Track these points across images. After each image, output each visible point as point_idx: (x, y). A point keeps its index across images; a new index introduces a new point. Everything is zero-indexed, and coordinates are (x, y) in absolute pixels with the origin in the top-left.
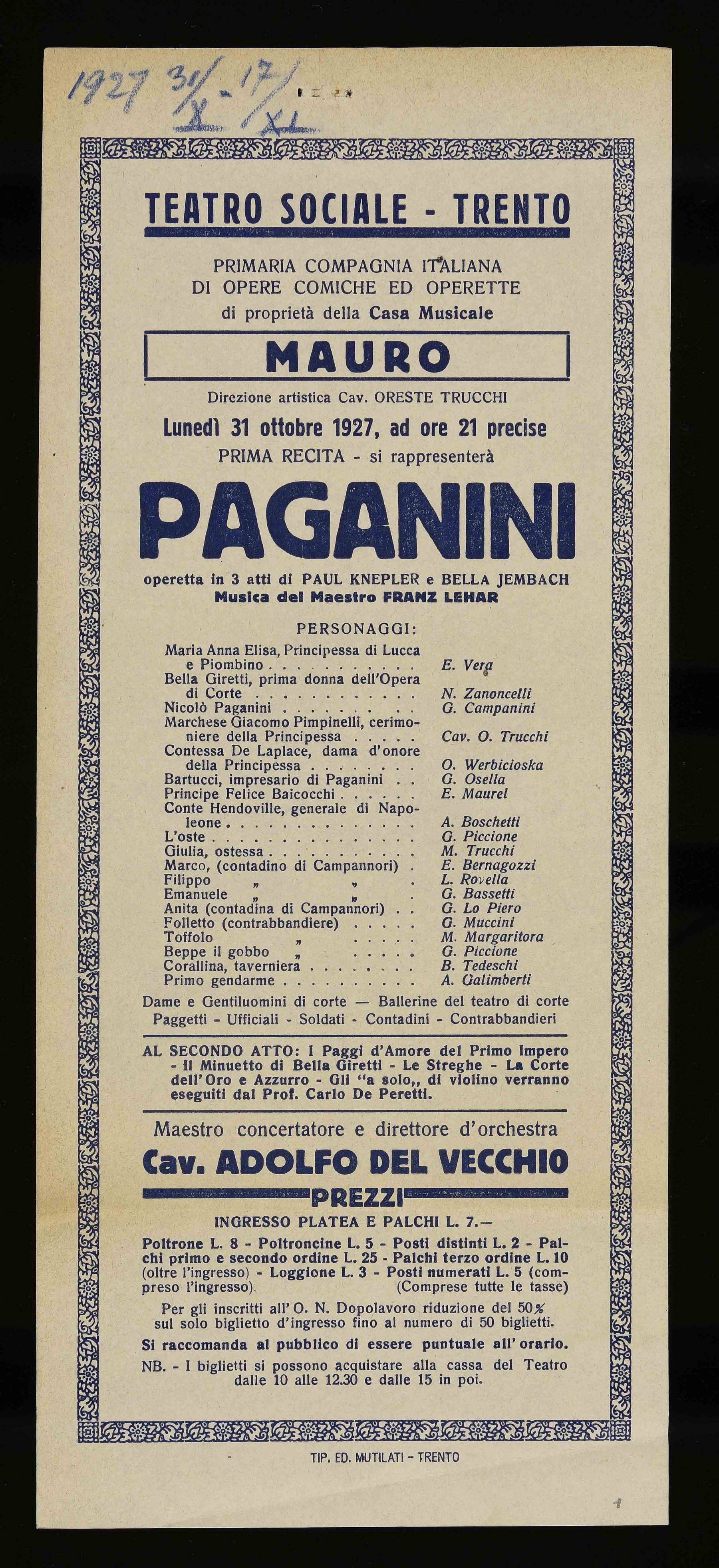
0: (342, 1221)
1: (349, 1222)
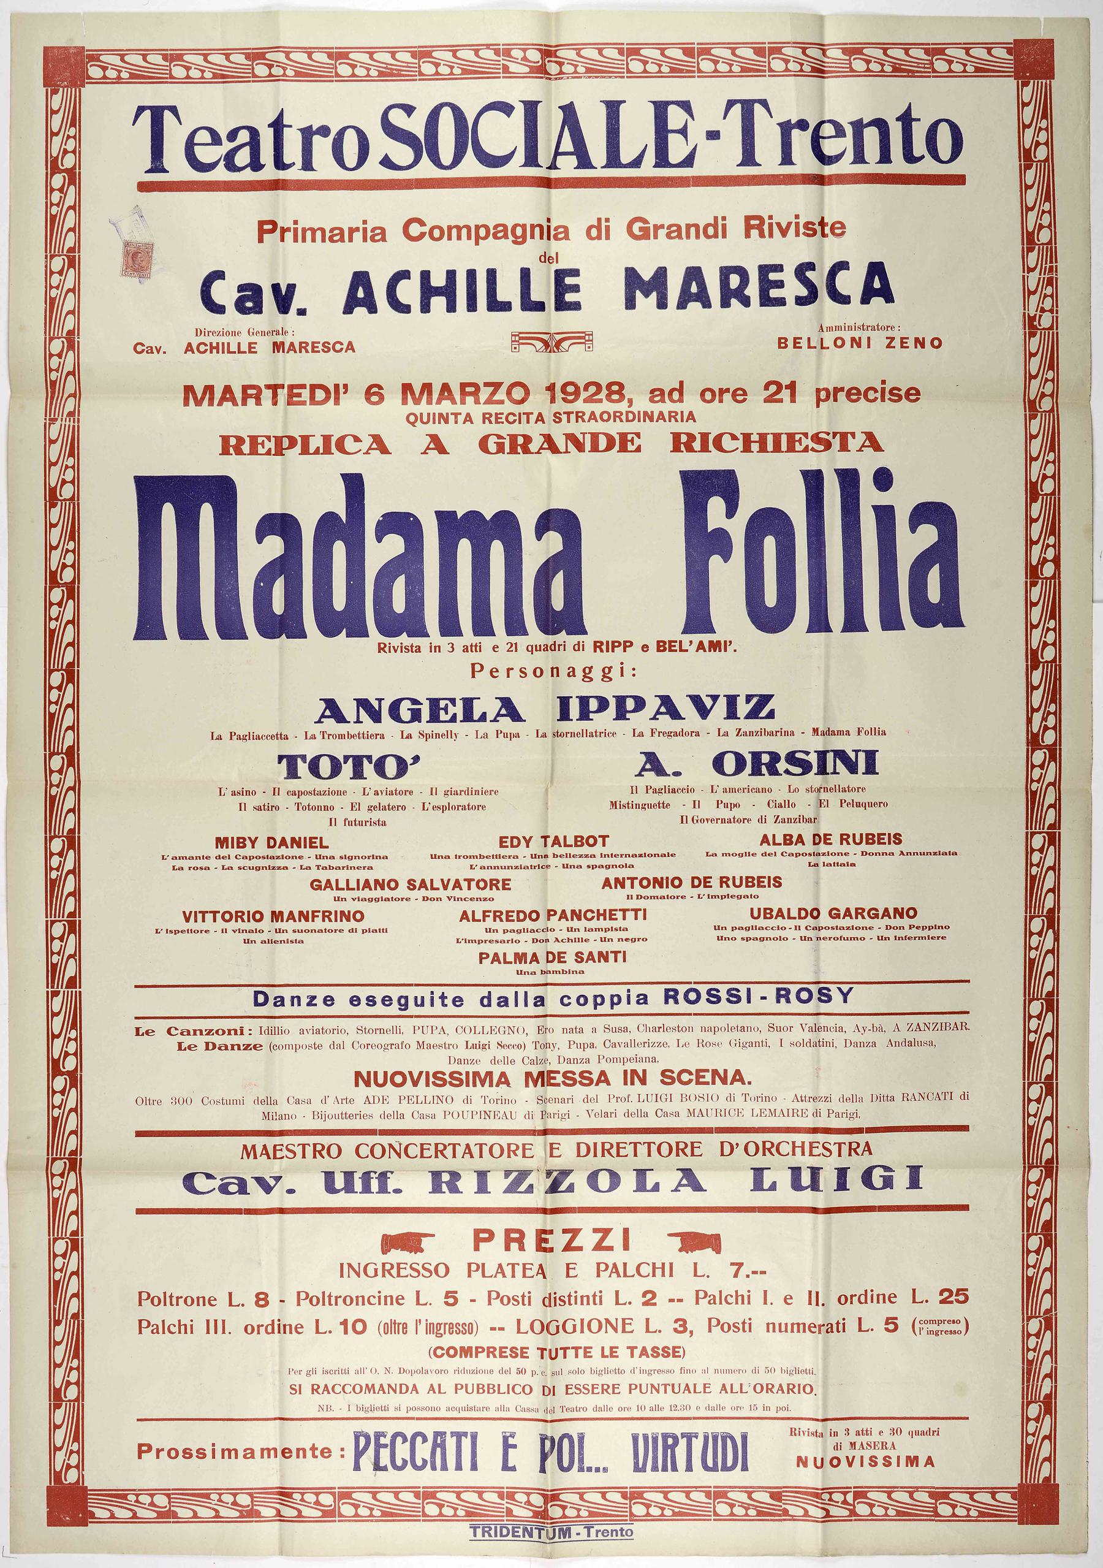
0: (524, 1269)
1: (536, 1268)
